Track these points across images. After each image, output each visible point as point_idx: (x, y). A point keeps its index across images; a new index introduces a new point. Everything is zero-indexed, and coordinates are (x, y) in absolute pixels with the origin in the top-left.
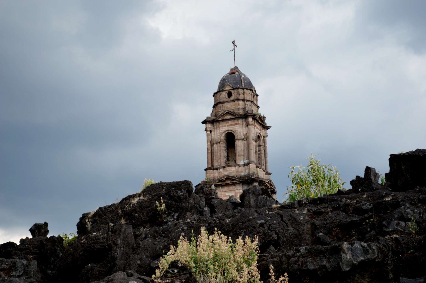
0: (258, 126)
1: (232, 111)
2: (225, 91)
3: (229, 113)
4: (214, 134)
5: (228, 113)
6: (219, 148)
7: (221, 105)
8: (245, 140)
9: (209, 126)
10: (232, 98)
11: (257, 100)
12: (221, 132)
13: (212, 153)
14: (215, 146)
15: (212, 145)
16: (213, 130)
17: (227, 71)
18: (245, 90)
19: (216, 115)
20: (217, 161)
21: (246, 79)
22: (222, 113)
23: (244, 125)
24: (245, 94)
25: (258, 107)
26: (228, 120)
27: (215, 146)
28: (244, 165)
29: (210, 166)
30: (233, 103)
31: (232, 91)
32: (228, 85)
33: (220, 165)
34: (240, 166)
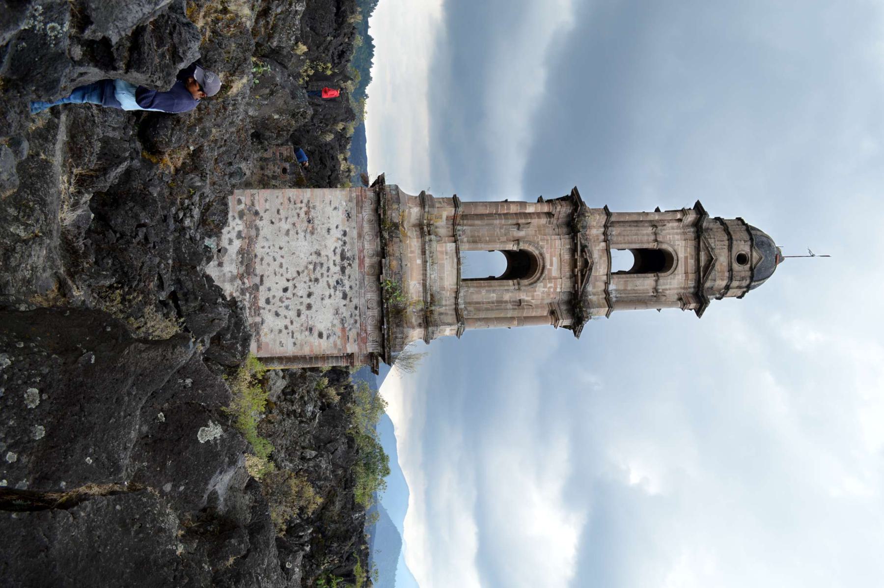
2: (751, 251)
4: (673, 228)
5: (711, 261)
7: (726, 243)
9: (691, 218)
10: (736, 266)
12: (677, 243)
14: (650, 228)
20: (619, 234)
26: (698, 260)
27: (650, 230)
28: (607, 292)
29: (613, 219)
30: (726, 269)
31: (749, 266)
32: (761, 258)
34: (607, 283)
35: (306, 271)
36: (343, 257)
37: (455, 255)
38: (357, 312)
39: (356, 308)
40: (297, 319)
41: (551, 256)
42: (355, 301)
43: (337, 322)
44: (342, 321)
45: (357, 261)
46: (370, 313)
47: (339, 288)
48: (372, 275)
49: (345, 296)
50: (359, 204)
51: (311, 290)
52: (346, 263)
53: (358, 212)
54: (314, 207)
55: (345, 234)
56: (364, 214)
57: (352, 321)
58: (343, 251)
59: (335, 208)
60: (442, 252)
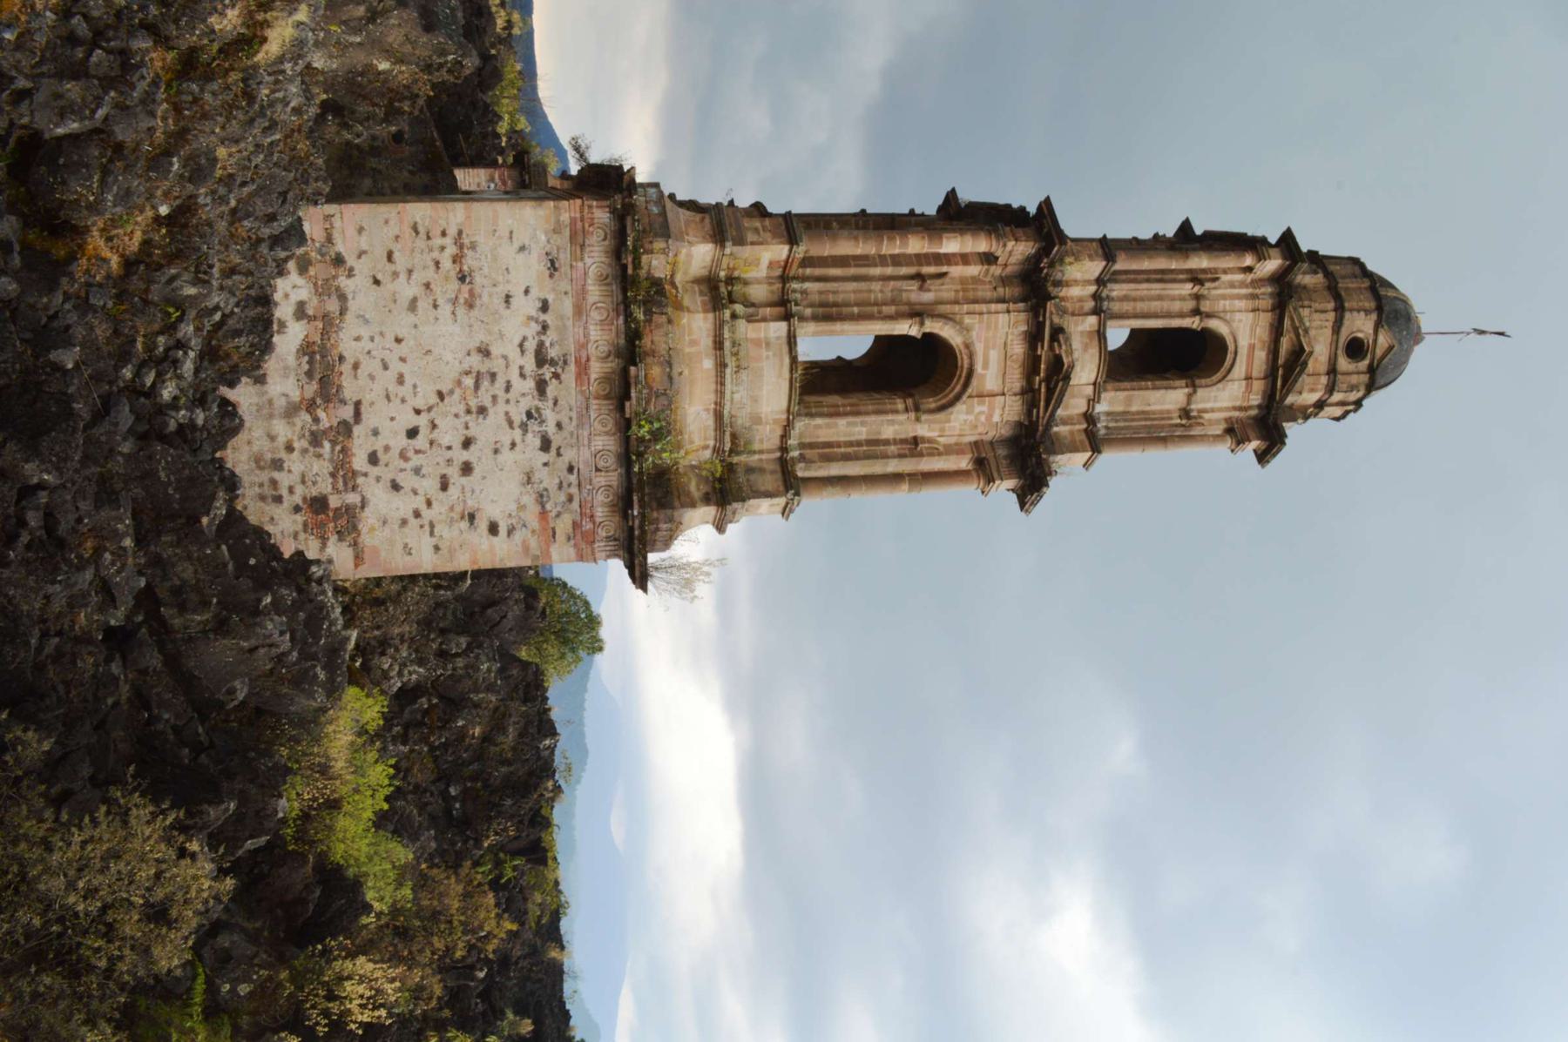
4: (1232, 285)
7: (1331, 316)
10: (1344, 363)
27: (1187, 288)
28: (1089, 418)
31: (1366, 362)
34: (1093, 400)
35: (458, 392)
36: (541, 359)
37: (785, 349)
38: (573, 478)
39: (571, 469)
40: (442, 495)
41: (986, 349)
42: (569, 455)
43: (529, 500)
44: (541, 498)
45: (572, 367)
46: (600, 480)
47: (534, 426)
48: (606, 397)
49: (546, 445)
50: (578, 238)
51: (470, 433)
52: (547, 372)
53: (574, 257)
54: (473, 247)
55: (545, 307)
56: (588, 261)
57: (562, 498)
58: (541, 345)
59: (522, 248)
60: (757, 343)
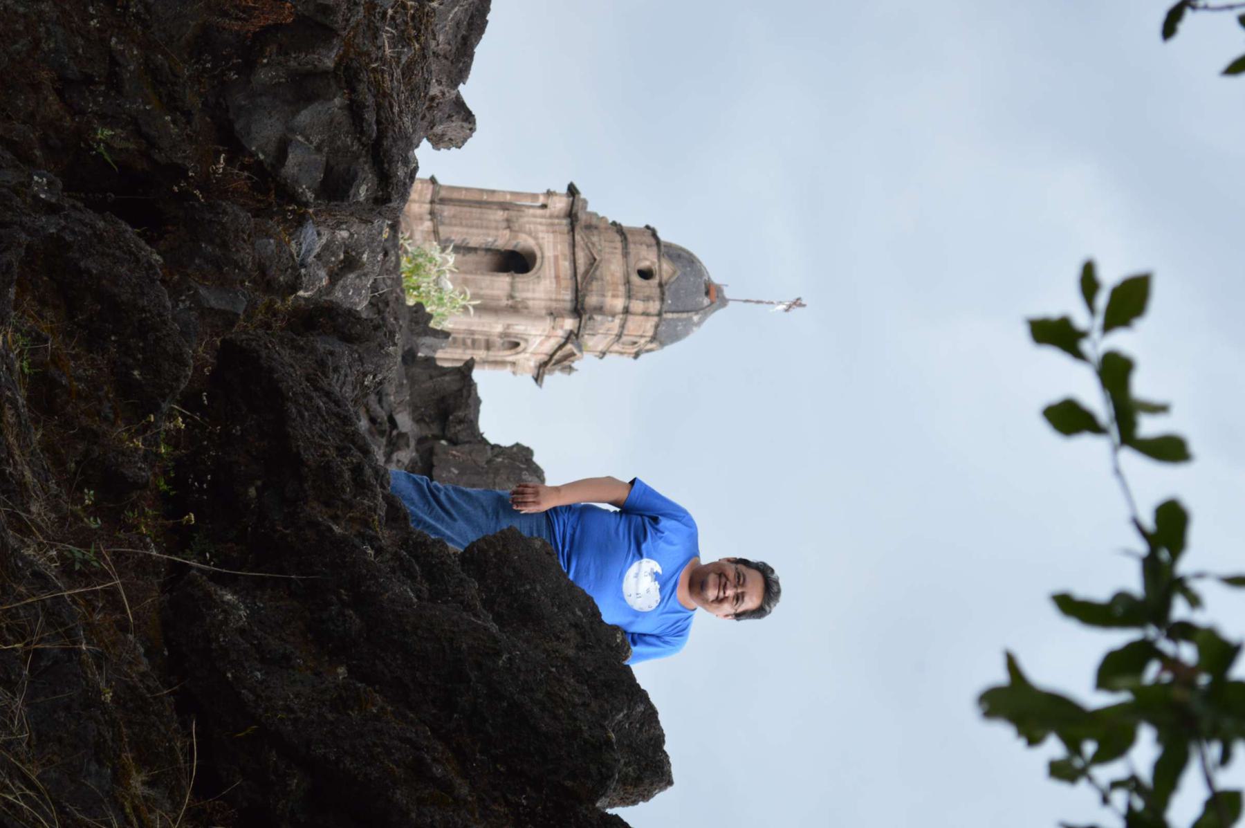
0: (552, 344)
1: (598, 273)
2: (659, 260)
3: (592, 264)
4: (535, 216)
5: (592, 262)
6: (494, 224)
7: (619, 245)
8: (510, 302)
9: (560, 204)
10: (636, 279)
11: (621, 353)
12: (541, 235)
13: (481, 204)
14: (500, 213)
15: (504, 206)
16: (547, 212)
17: (716, 278)
18: (656, 319)
19: (589, 227)
20: (454, 216)
21: (688, 327)
22: (593, 244)
23: (554, 305)
24: (642, 318)
25: (603, 354)
26: (574, 262)
27: (500, 215)
29: (443, 194)
30: (621, 281)
33: (443, 224)
